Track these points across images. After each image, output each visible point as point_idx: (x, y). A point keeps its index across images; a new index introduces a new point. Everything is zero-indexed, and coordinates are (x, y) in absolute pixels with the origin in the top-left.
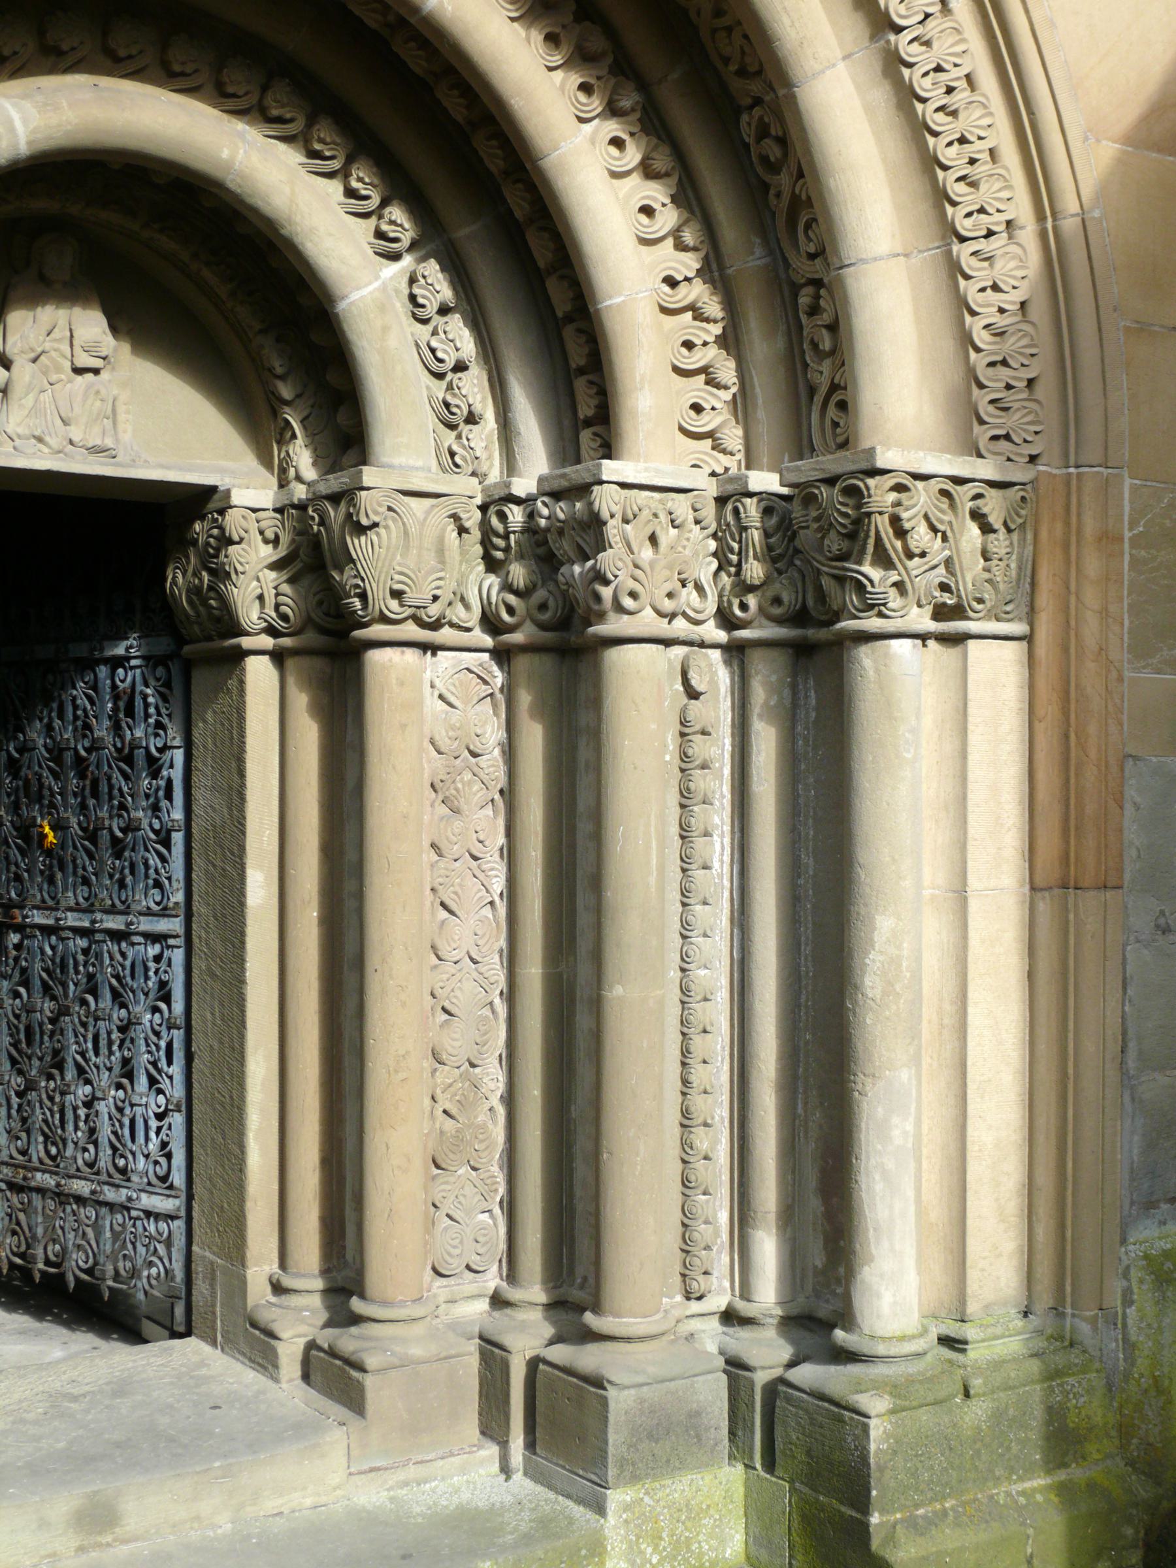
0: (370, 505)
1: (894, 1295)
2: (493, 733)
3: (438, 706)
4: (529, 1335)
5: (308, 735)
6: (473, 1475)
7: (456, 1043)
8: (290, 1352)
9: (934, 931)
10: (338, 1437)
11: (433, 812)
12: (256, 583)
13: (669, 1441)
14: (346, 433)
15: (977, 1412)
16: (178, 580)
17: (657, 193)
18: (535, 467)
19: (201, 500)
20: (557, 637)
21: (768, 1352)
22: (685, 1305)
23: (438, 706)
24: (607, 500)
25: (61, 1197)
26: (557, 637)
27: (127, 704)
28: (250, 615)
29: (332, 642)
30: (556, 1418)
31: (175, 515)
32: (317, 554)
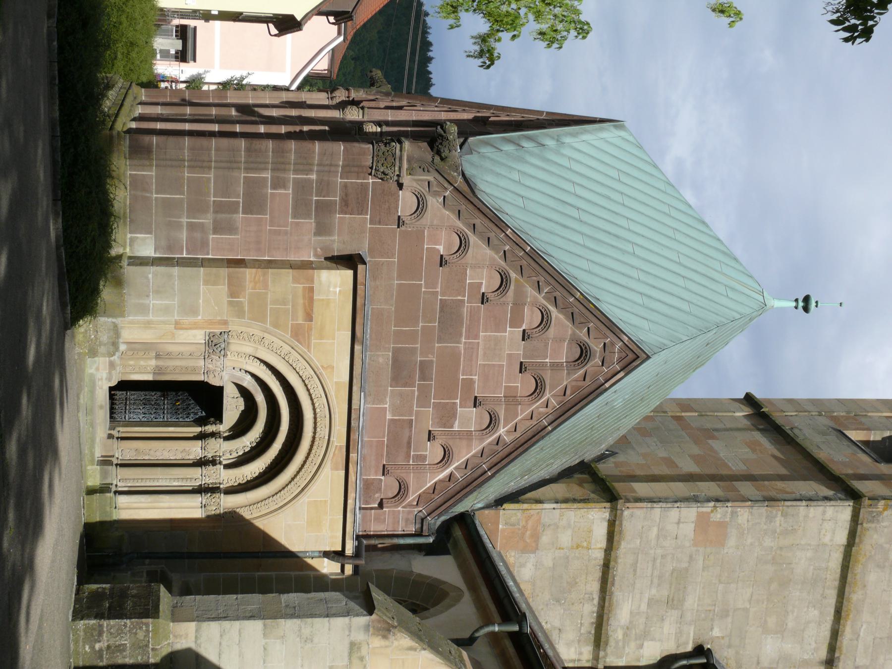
0: (218, 440)
1: (122, 500)
2: (191, 457)
3: (195, 450)
4: (115, 462)
5: (191, 435)
6: (98, 453)
7: (152, 452)
8: (112, 432)
9: (166, 505)
10: (106, 436)
11: (181, 449)
12: (210, 428)
13: (104, 474)
14: (227, 439)
15: (108, 509)
16: (212, 419)
17: (257, 474)
18: (225, 462)
19: (221, 422)
20: (201, 463)
21: (114, 489)
22: (122, 479)
23: (195, 450)
24: (218, 466)
25: (126, 404)
26: (201, 463)
27: (196, 414)
28: (207, 428)
29: (201, 437)
30: (106, 462)
31: (219, 418)
32: (213, 435)
